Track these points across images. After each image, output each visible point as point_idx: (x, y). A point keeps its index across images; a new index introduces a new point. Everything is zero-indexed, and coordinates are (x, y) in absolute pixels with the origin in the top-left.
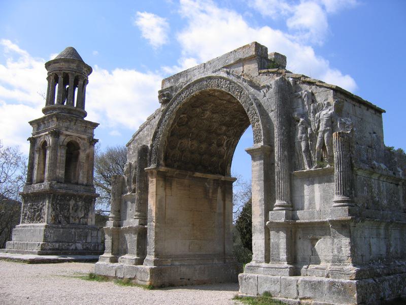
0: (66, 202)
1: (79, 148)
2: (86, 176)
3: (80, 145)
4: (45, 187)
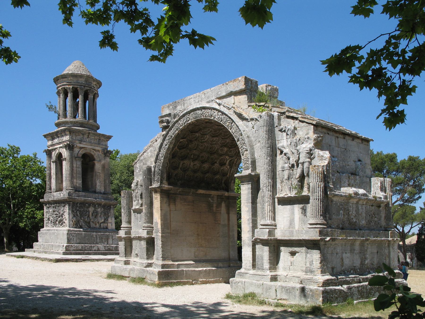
0: (86, 209)
4: (64, 195)
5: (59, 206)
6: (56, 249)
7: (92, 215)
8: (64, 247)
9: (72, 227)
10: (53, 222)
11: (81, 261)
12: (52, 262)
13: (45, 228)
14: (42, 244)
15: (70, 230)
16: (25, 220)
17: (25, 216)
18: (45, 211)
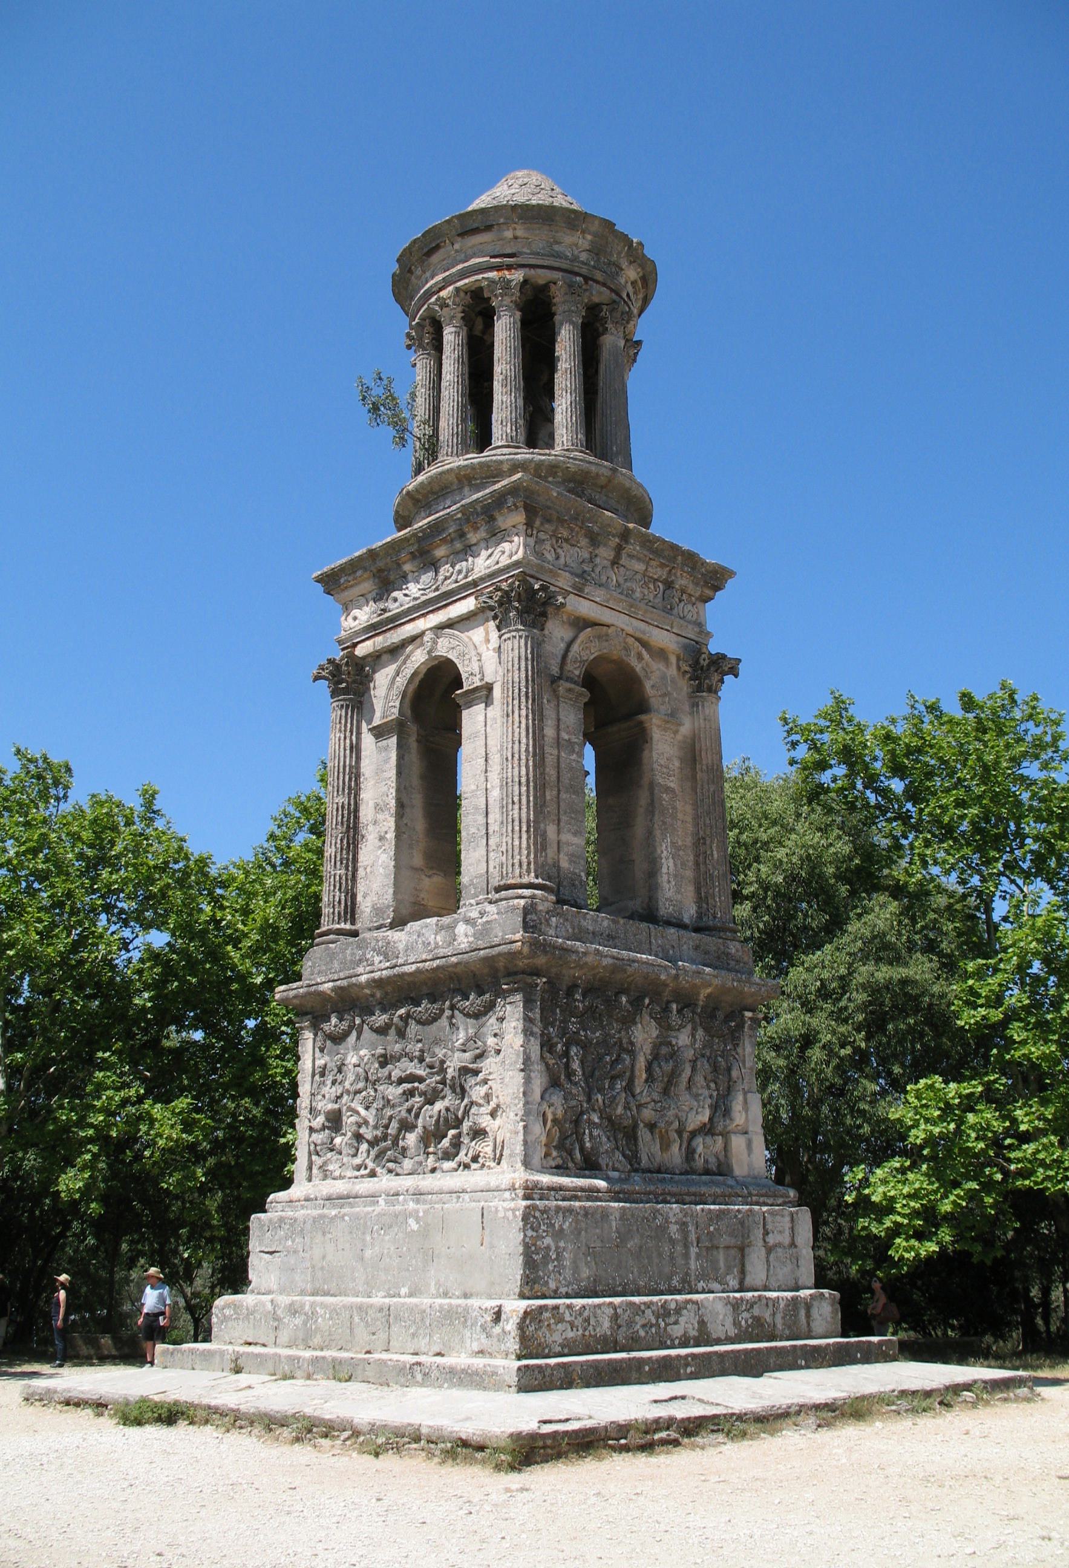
1: (643, 707)
2: (689, 873)
3: (648, 685)
5: (435, 1019)
6: (422, 1343)
7: (650, 1079)
8: (510, 1325)
9: (543, 1170)
10: (372, 1144)
11: (676, 1443)
12: (470, 1461)
13: (296, 1191)
14: (293, 1310)
15: (536, 1186)
16: (88, 1157)
17: (91, 1132)
18: (306, 1064)
